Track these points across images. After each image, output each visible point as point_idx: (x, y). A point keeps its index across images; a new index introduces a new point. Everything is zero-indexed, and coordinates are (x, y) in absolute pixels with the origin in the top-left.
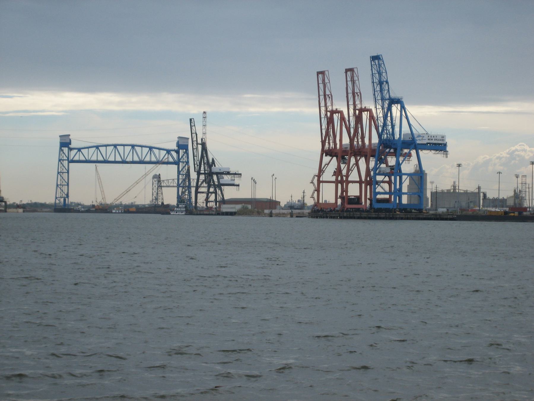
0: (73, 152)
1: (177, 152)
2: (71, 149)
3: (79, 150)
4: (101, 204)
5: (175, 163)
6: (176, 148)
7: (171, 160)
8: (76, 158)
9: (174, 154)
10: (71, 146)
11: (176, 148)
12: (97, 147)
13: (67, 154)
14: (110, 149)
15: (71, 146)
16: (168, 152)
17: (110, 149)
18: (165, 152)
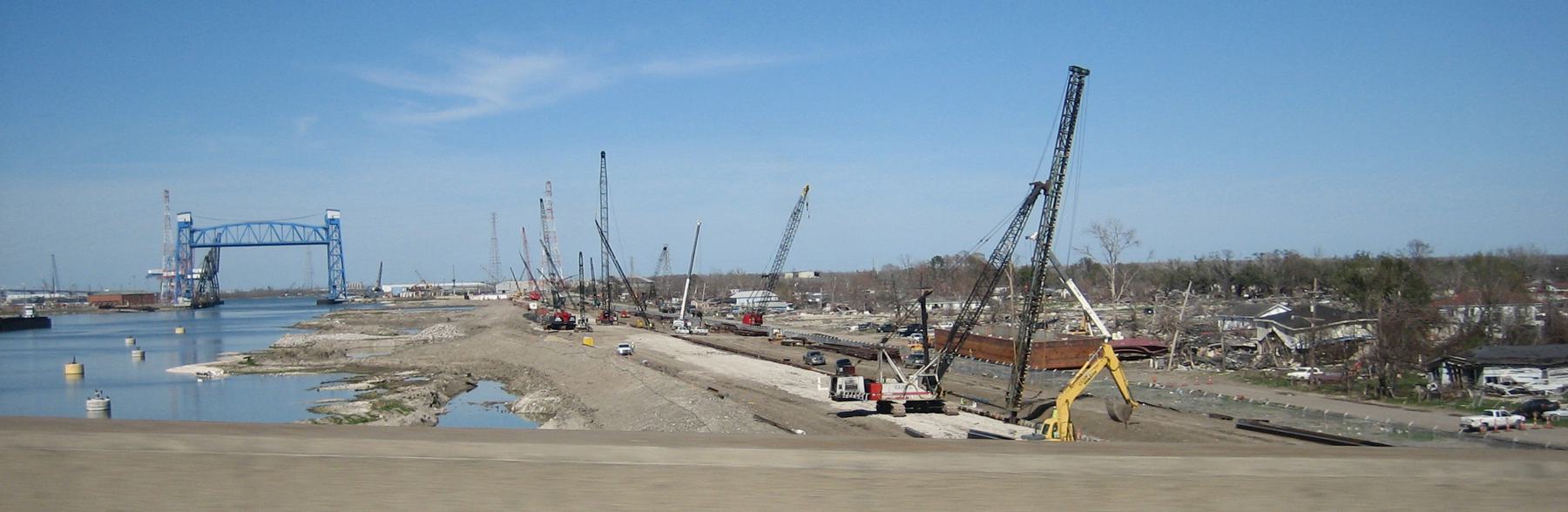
0: (196, 235)
1: (325, 229)
2: (192, 232)
3: (203, 232)
4: (255, 290)
5: (325, 244)
6: (324, 224)
7: (319, 239)
8: (200, 242)
9: (323, 232)
10: (194, 227)
11: (324, 224)
12: (248, 225)
13: (188, 236)
14: (242, 228)
15: (194, 227)
16: (316, 230)
17: (288, 228)
18: (312, 230)
